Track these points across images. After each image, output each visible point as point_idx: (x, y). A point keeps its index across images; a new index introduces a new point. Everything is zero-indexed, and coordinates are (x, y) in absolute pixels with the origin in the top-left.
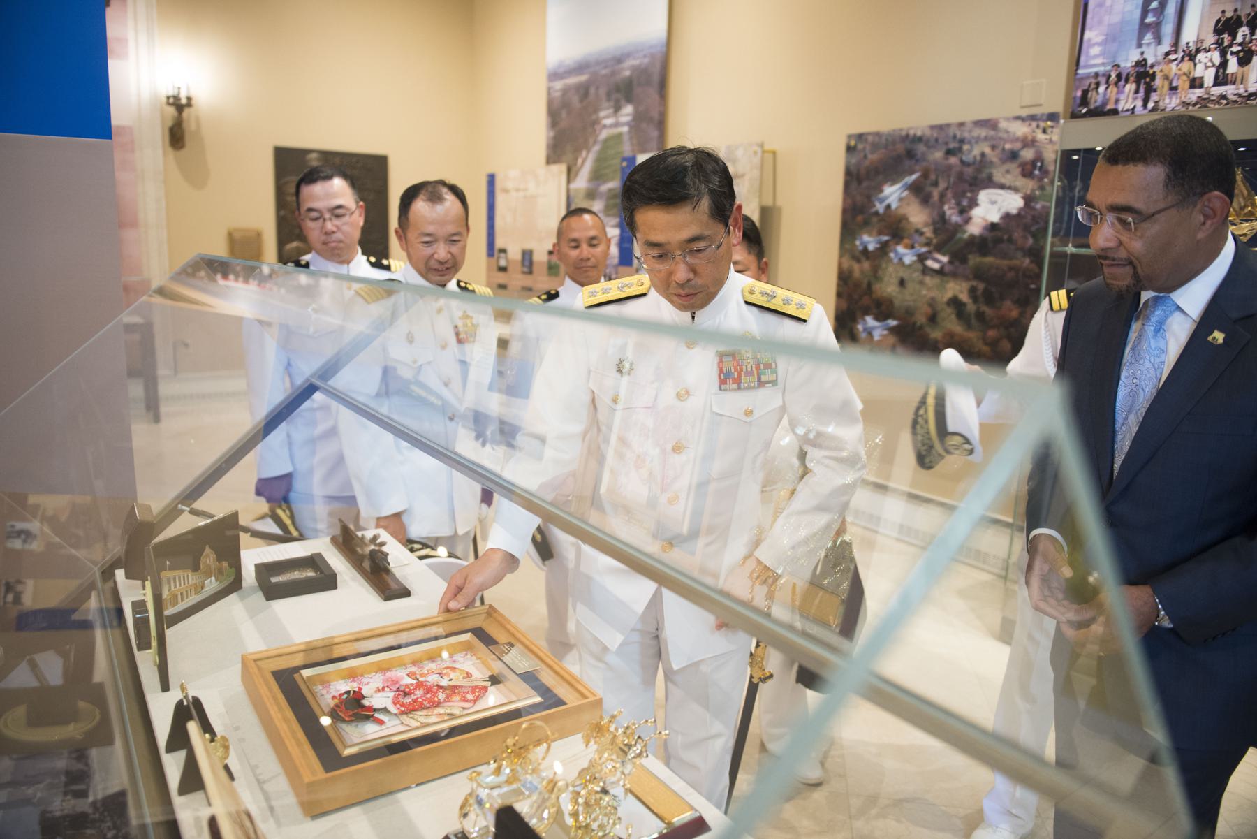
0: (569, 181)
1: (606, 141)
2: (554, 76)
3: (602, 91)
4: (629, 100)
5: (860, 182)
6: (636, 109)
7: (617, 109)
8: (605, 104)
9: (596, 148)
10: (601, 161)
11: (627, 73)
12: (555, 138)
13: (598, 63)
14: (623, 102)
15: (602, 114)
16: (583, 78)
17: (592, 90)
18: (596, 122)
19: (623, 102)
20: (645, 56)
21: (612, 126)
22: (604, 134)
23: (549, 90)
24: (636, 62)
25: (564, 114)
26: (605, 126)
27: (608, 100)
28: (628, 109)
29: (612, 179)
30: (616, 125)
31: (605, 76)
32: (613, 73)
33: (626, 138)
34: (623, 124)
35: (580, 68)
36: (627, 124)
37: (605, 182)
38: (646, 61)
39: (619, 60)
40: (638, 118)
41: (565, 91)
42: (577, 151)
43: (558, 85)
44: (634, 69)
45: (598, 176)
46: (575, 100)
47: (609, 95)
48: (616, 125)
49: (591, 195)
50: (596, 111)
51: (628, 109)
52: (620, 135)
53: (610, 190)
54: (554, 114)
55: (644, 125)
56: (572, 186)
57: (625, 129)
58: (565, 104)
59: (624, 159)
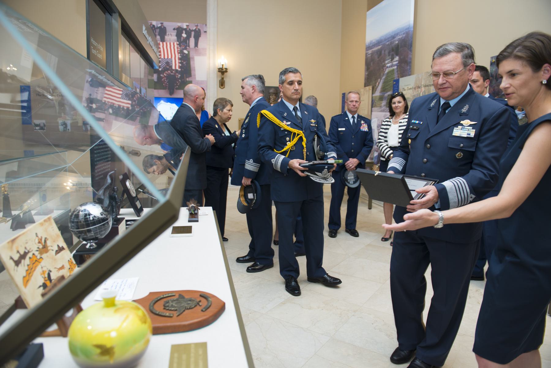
0: (373, 94)
1: (388, 73)
2: (368, 48)
3: (387, 52)
4: (397, 55)
5: (497, 80)
6: (400, 58)
7: (392, 59)
8: (388, 58)
9: (384, 77)
10: (384, 83)
11: (397, 42)
12: (368, 75)
13: (385, 40)
14: (395, 55)
15: (386, 62)
16: (379, 47)
17: (383, 52)
18: (384, 66)
19: (395, 55)
20: (404, 34)
21: (390, 67)
22: (387, 71)
23: (366, 54)
24: (400, 37)
25: (372, 64)
26: (387, 67)
27: (389, 55)
28: (397, 58)
29: (389, 91)
30: (392, 66)
31: (388, 45)
32: (391, 43)
33: (395, 71)
34: (394, 65)
35: (378, 43)
36: (396, 65)
37: (387, 92)
38: (404, 35)
39: (393, 37)
40: (400, 61)
41: (372, 54)
42: (376, 80)
43: (370, 52)
44: (399, 40)
45: (384, 90)
46: (376, 57)
47: (389, 53)
48: (392, 66)
49: (381, 98)
50: (384, 61)
51: (397, 58)
52: (393, 70)
53: (389, 95)
54: (368, 64)
55: (403, 65)
56: (374, 95)
57: (396, 67)
58: (372, 60)
59: (394, 81)
